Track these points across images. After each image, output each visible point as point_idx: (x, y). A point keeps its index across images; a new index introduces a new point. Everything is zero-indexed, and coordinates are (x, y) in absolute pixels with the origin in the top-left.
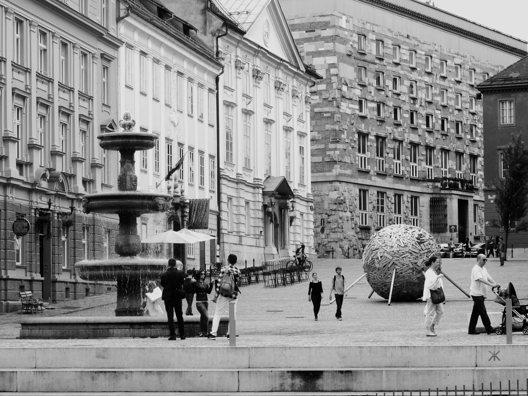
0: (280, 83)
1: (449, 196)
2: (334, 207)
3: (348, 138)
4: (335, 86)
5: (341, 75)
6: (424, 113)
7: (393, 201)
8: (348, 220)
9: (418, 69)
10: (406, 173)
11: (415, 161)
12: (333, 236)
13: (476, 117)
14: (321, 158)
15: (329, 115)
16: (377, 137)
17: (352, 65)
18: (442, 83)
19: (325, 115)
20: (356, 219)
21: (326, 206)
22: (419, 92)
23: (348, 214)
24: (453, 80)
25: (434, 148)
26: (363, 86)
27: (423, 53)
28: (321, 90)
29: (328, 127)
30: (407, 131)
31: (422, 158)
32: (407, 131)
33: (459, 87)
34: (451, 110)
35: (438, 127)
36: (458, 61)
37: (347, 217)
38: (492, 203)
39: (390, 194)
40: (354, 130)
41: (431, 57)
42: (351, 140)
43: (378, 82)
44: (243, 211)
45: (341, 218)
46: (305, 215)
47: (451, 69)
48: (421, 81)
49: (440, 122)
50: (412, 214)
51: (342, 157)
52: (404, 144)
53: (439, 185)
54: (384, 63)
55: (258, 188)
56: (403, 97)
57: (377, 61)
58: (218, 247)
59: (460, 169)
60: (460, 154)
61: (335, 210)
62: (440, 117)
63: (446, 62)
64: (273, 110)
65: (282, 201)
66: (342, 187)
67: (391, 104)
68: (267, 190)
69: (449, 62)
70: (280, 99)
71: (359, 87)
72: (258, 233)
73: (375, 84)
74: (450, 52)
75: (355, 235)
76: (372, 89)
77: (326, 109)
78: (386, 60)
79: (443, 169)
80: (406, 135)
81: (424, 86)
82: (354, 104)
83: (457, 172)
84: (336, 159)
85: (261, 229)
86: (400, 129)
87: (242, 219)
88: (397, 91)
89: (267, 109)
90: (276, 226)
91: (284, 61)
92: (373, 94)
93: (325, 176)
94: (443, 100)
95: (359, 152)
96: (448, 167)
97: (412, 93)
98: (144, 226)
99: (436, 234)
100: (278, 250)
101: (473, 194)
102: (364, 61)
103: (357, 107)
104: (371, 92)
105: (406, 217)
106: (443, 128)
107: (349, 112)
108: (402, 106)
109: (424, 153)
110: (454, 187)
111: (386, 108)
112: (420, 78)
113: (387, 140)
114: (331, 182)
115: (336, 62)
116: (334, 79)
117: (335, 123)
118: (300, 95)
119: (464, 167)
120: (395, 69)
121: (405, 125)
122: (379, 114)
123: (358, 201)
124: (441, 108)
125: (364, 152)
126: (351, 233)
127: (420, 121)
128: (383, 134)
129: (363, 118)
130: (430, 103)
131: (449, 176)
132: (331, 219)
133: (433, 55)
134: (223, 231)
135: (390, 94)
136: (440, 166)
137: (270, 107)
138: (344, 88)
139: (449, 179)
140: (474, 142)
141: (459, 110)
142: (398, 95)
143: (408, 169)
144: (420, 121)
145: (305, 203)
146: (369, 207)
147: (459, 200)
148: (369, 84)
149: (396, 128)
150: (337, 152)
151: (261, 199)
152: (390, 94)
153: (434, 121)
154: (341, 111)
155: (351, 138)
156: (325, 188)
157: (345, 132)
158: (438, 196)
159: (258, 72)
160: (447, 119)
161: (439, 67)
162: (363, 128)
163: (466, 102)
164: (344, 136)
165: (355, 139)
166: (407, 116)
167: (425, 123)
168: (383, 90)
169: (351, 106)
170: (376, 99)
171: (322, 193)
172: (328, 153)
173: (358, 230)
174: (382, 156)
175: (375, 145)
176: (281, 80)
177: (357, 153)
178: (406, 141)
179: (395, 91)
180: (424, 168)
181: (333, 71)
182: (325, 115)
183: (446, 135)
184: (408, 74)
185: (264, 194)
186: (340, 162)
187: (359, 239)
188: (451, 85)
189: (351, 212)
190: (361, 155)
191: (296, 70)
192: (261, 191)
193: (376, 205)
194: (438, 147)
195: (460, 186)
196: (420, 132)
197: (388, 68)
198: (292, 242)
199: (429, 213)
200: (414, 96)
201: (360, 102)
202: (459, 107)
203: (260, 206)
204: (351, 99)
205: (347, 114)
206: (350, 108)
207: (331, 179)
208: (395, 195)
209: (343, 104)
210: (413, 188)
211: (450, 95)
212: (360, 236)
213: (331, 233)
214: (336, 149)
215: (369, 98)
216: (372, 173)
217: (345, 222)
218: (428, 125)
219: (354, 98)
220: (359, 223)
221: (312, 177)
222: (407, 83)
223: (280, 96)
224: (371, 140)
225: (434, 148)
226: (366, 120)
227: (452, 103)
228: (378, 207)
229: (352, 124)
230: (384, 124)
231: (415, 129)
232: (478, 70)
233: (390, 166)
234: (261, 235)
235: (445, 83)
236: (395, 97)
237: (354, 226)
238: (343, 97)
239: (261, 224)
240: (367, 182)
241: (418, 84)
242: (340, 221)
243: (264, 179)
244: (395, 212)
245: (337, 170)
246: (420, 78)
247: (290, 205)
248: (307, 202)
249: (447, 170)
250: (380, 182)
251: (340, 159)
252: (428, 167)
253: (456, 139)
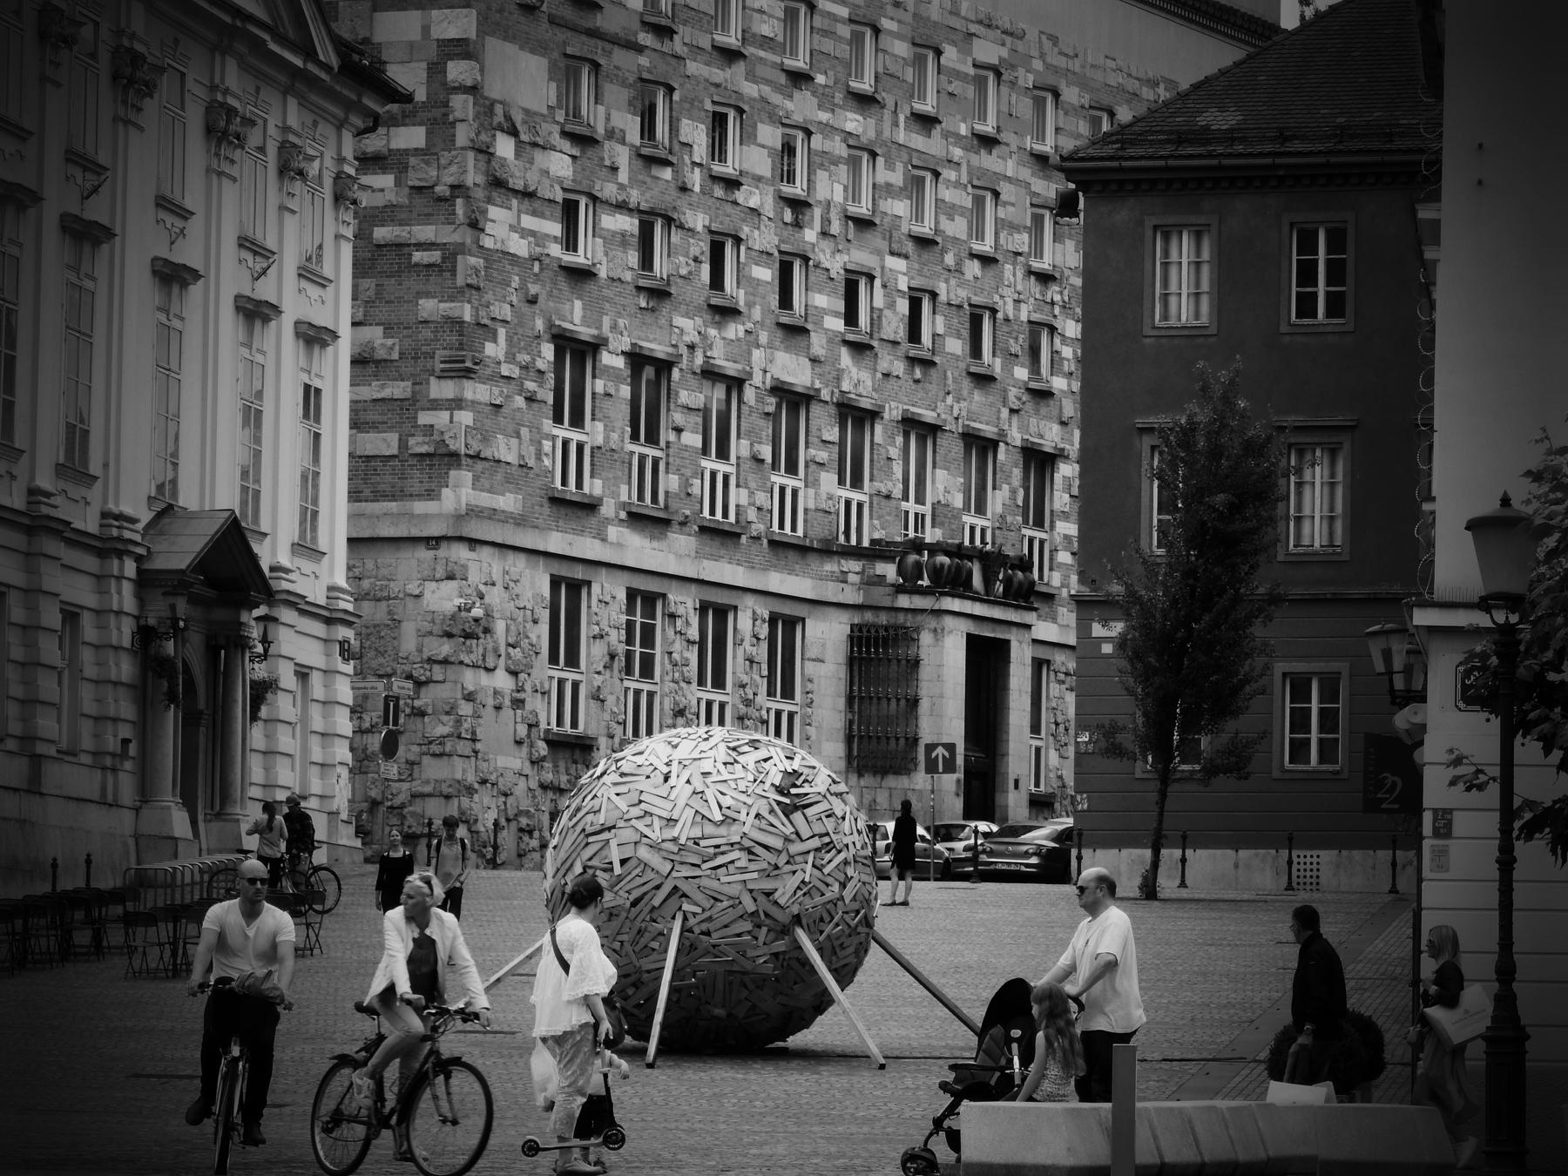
0: (231, 112)
1: (932, 622)
2: (445, 648)
3: (511, 358)
4: (463, 135)
5: (493, 90)
6: (835, 263)
7: (694, 633)
8: (498, 708)
9: (820, 79)
10: (752, 515)
11: (792, 469)
12: (434, 770)
13: (1053, 292)
14: (393, 438)
15: (434, 256)
16: (637, 359)
17: (539, 48)
18: (918, 141)
19: (417, 256)
20: (535, 704)
21: (408, 643)
22: (821, 175)
23: (502, 681)
24: (963, 130)
25: (874, 415)
26: (584, 141)
27: (843, 12)
28: (406, 152)
29: (429, 307)
30: (764, 337)
31: (822, 456)
32: (764, 337)
33: (989, 161)
34: (949, 259)
35: (894, 326)
36: (988, 51)
37: (496, 693)
38: (1107, 656)
39: (684, 602)
40: (540, 324)
41: (877, 31)
42: (525, 368)
43: (648, 129)
44: (50, 650)
45: (469, 697)
46: (316, 679)
47: (955, 87)
48: (829, 129)
49: (903, 306)
50: (771, 693)
51: (485, 440)
52: (749, 394)
53: (889, 571)
54: (678, 46)
55: (120, 554)
56: (750, 197)
57: (646, 39)
59: (981, 510)
60: (980, 446)
61: (445, 662)
62: (903, 285)
63: (938, 53)
64: (195, 226)
65: (220, 614)
66: (481, 565)
67: (698, 220)
68: (159, 563)
69: (950, 55)
70: (226, 182)
71: (566, 145)
72: (112, 744)
73: (634, 136)
74: (955, 13)
75: (528, 769)
76: (622, 156)
77: (425, 232)
78: (684, 33)
79: (911, 506)
80: (757, 355)
81: (839, 148)
82: (542, 215)
83: (968, 520)
84: (458, 445)
85: (125, 731)
86: (734, 330)
87: (48, 686)
88: (728, 169)
89: (170, 219)
90: (190, 722)
91: (250, 18)
92: (623, 176)
93: (412, 516)
94: (918, 216)
95: (558, 419)
96: (929, 499)
97: (791, 178)
99: (868, 780)
100: (194, 823)
101: (1029, 618)
102: (594, 33)
103: (555, 228)
104: (614, 169)
105: (748, 703)
106: (914, 334)
107: (520, 247)
108: (745, 231)
109: (832, 434)
110: (955, 583)
111: (676, 237)
112: (824, 116)
113: (676, 374)
114: (433, 542)
115: (473, 35)
116: (462, 105)
117: (457, 294)
118: (313, 169)
119: (997, 500)
120: (718, 74)
121: (757, 313)
122: (647, 261)
123: (544, 629)
124: (910, 247)
125: (577, 421)
126: (511, 761)
127: (820, 300)
128: (660, 350)
129: (581, 276)
130: (864, 224)
131: (931, 535)
132: (426, 699)
133: (886, 24)
135: (696, 179)
136: (897, 492)
137: (185, 214)
138: (505, 147)
139: (934, 549)
140: (1043, 395)
141: (987, 261)
142: (732, 184)
143: (761, 498)
144: (820, 300)
145: (318, 628)
146: (594, 654)
147: (968, 635)
148: (610, 134)
149: (719, 326)
150: (465, 418)
151: (129, 602)
152: (696, 179)
153: (879, 301)
154: (488, 243)
155: (524, 358)
156: (407, 567)
157: (502, 333)
158: (883, 619)
159: (137, 59)
160: (934, 295)
161: (909, 73)
162: (576, 318)
163: (1014, 228)
164: (494, 350)
165: (540, 364)
166: (765, 274)
167: (840, 306)
168: (666, 163)
169: (528, 222)
170: (635, 196)
171: (395, 587)
172: (424, 418)
173: (542, 748)
174: (652, 439)
175: (625, 391)
176: (231, 101)
177: (548, 425)
178: (757, 379)
179: (717, 168)
180: (830, 498)
181: (458, 71)
182: (417, 256)
183: (927, 364)
184: (776, 99)
185: (146, 581)
186: (477, 457)
187: (544, 787)
188: (957, 153)
189: (514, 674)
190: (562, 433)
191: (298, 62)
192: (130, 568)
193: (621, 649)
194: (893, 411)
195: (977, 581)
196: (818, 344)
197: (693, 67)
198: (255, 792)
199: (842, 687)
200: (797, 190)
201: (569, 212)
202: (986, 247)
203: (125, 633)
204: (528, 195)
205: (513, 258)
206: (525, 233)
207: (435, 530)
208: (703, 609)
209: (494, 212)
210: (779, 582)
211: (947, 195)
212: (548, 777)
213: (426, 760)
214: (457, 404)
215: (609, 191)
216: (608, 509)
217: (489, 713)
218: (851, 317)
219: (546, 192)
220: (546, 717)
221: (353, 517)
222: (770, 135)
223: (225, 167)
224: (610, 372)
225: (874, 415)
226: (591, 286)
227: (957, 228)
228: (629, 656)
229: (533, 301)
230: (665, 308)
231: (795, 332)
232: (1071, 94)
233: (686, 484)
234: (124, 755)
235: (931, 145)
236: (719, 192)
237: (522, 731)
238: (497, 183)
239: (127, 710)
240: (588, 548)
241: (817, 142)
242: (465, 709)
243: (145, 516)
244: (701, 682)
245: (460, 491)
246: (824, 116)
247: (255, 632)
248: (329, 621)
249: (927, 509)
250: (639, 549)
251: (475, 446)
252: (846, 493)
253: (966, 383)
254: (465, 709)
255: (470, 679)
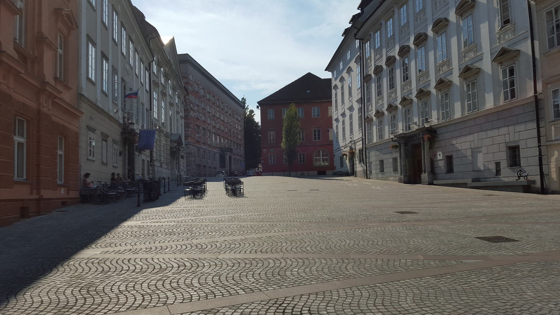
23: (193, 159)
45: (191, 161)
58: (151, 168)
68: (172, 139)
72: (168, 162)
98: (104, 142)
134: (154, 159)
185: (171, 141)
189: (194, 158)
240: (200, 146)
242: (190, 162)
250: (204, 147)
254: (190, 162)
255: (191, 159)
